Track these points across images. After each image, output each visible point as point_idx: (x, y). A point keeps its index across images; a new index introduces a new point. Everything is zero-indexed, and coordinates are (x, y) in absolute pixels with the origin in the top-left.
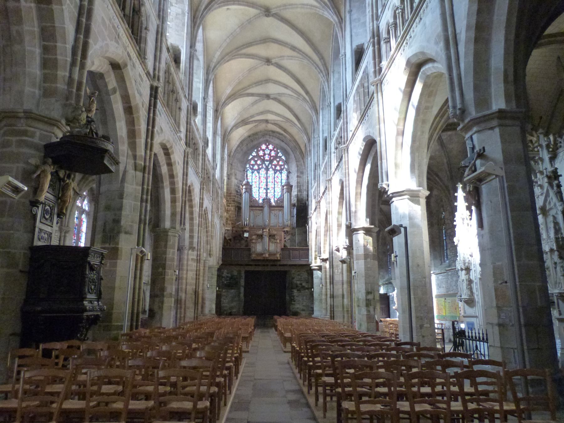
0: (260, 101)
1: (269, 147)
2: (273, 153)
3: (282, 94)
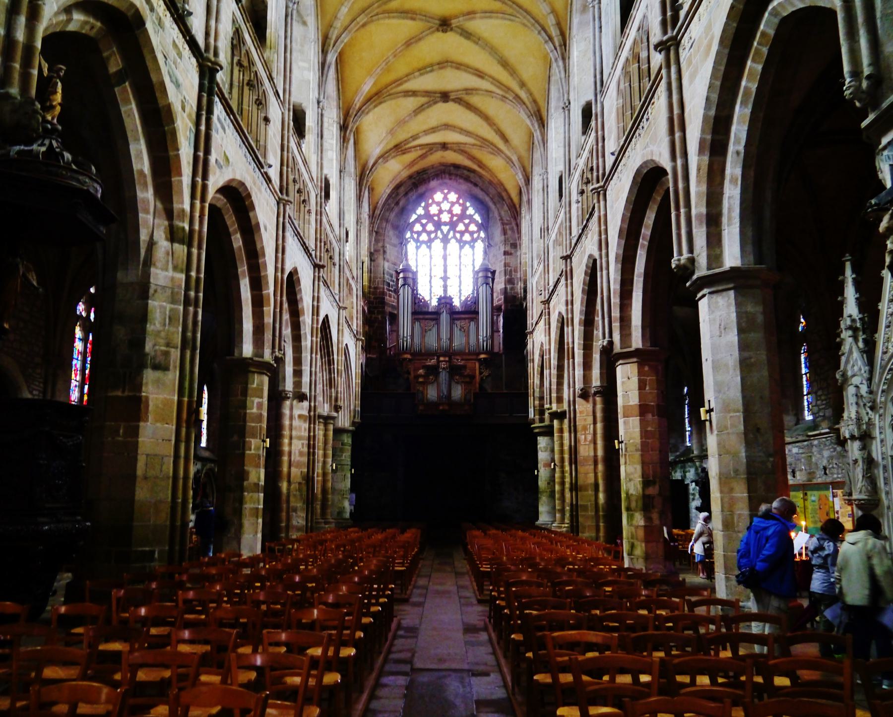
0: (430, 106)
2: (457, 210)
3: (472, 90)
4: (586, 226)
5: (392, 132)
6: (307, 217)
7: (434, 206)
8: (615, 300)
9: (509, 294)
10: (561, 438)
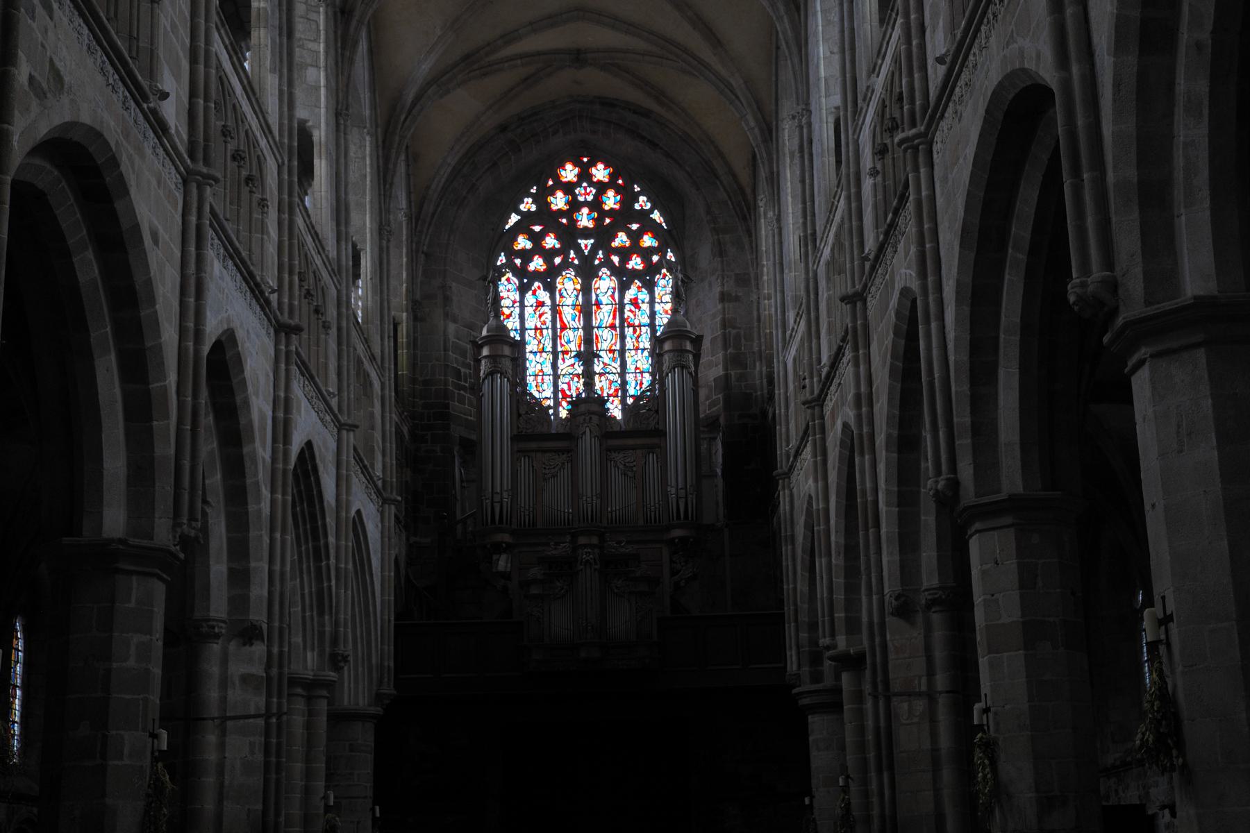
1: (593, 171)
4: (892, 226)
7: (560, 194)
8: (960, 388)
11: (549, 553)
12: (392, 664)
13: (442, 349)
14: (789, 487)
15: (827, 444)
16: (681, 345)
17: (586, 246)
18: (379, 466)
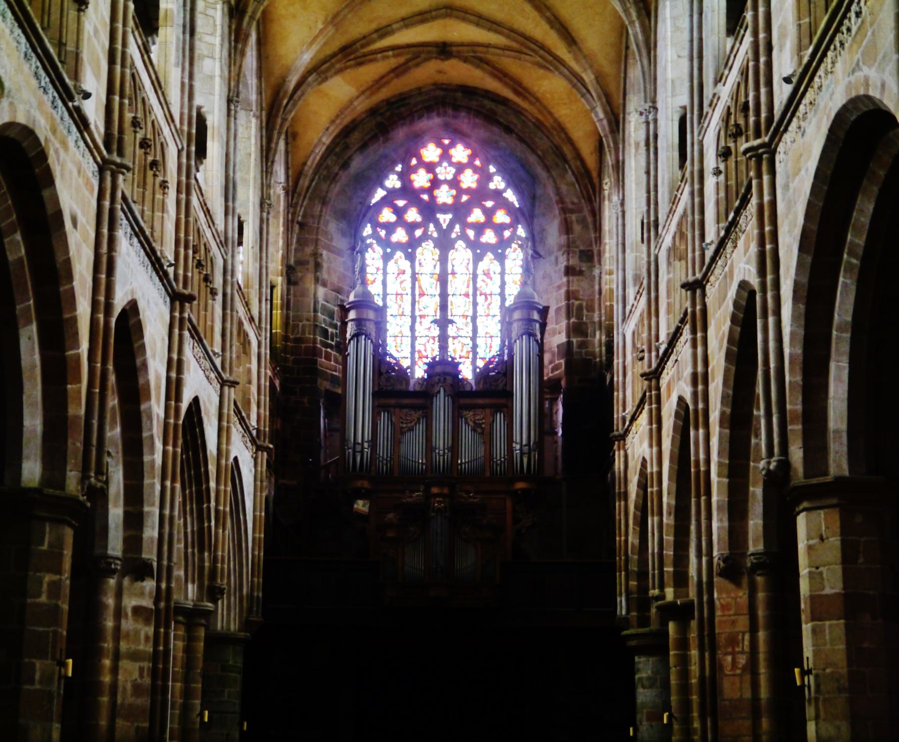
1: (452, 152)
2: (469, 179)
4: (734, 223)
5: (335, 20)
6: (159, 196)
7: (422, 172)
9: (576, 357)
10: (684, 660)
11: (404, 501)
12: (261, 595)
13: (312, 310)
14: (624, 448)
15: (663, 413)
16: (529, 315)
17: (445, 221)
18: (254, 417)
